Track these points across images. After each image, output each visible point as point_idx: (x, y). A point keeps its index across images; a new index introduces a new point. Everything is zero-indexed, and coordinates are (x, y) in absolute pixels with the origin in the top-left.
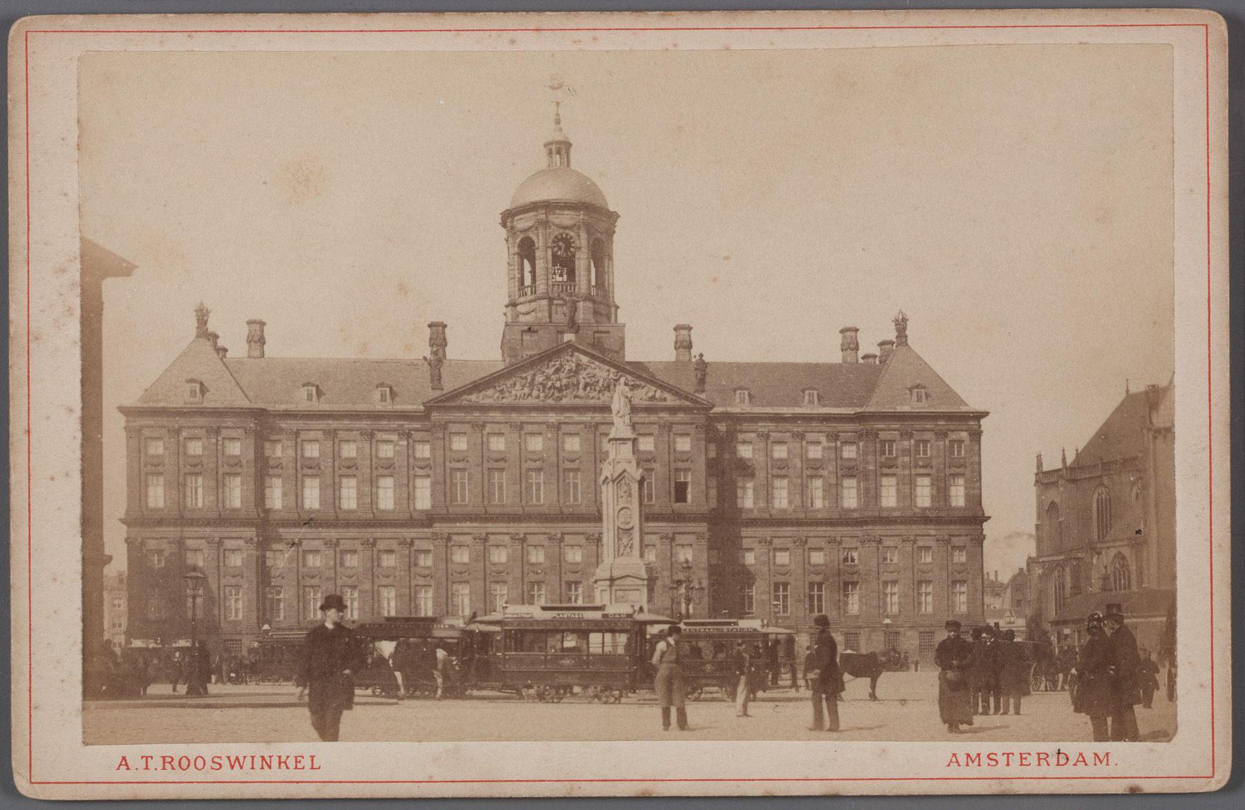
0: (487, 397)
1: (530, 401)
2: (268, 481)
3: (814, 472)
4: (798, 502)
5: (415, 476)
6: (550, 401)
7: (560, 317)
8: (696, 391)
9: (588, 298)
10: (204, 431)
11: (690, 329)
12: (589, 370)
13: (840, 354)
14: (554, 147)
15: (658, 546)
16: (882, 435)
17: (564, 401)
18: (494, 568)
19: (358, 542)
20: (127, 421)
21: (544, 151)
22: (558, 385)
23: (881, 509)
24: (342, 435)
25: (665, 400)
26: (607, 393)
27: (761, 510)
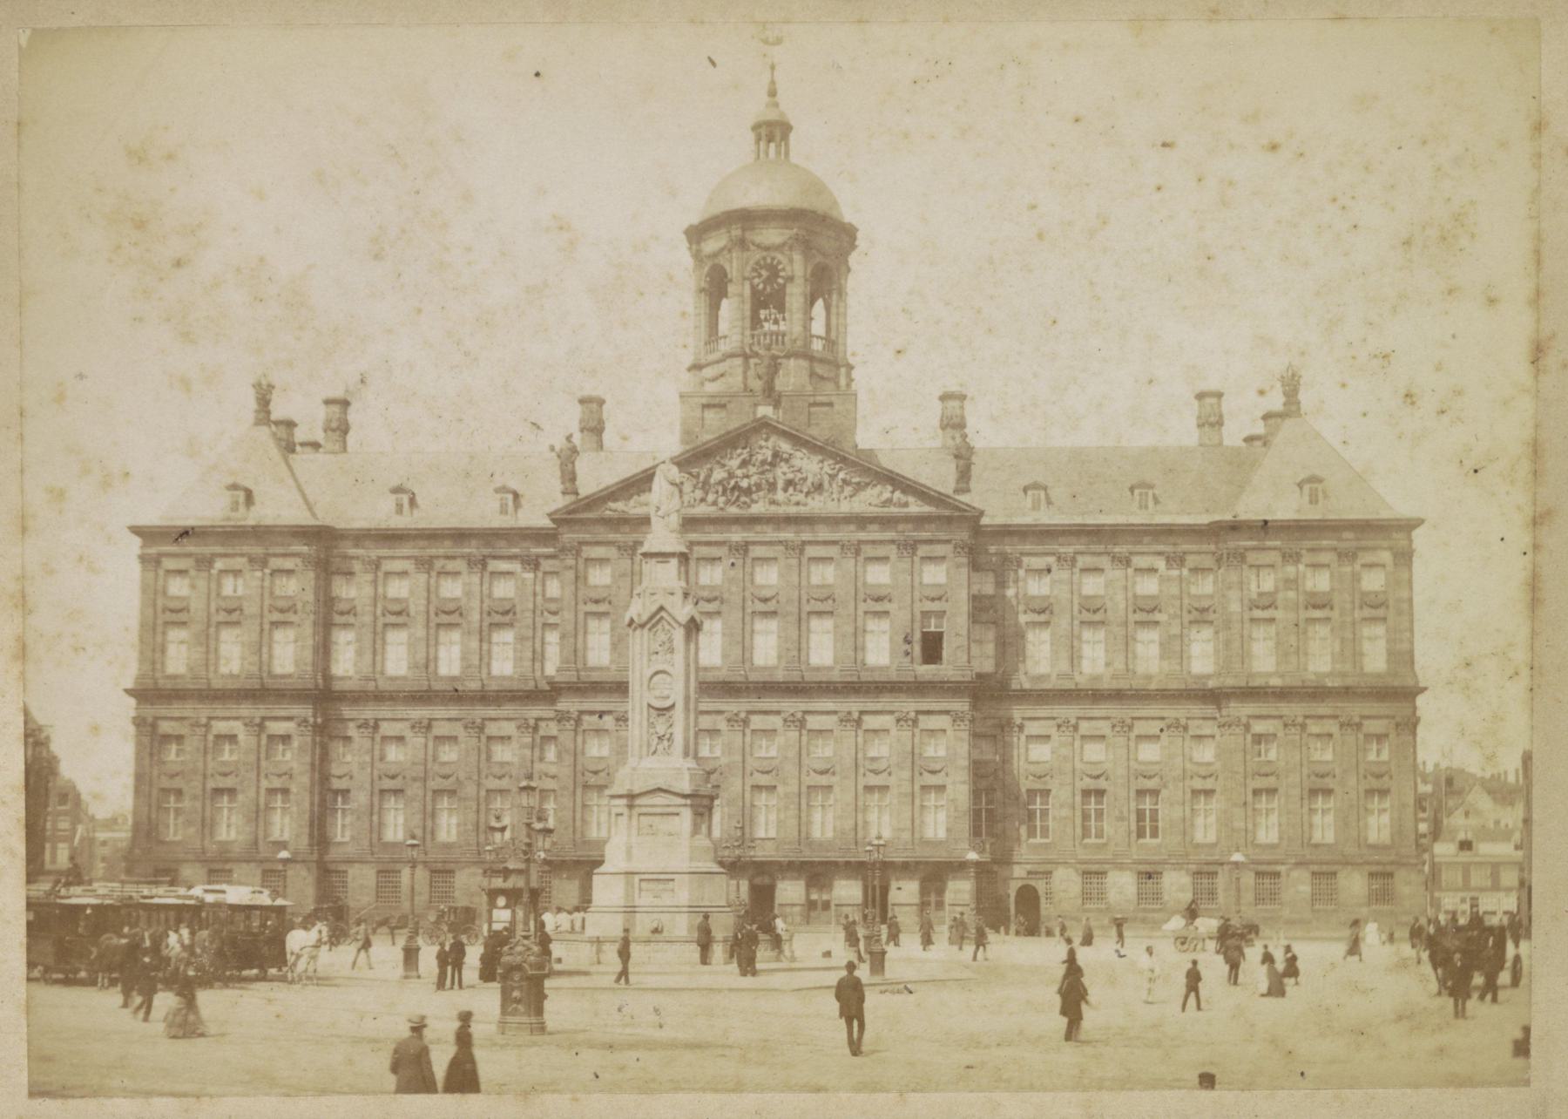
1: (701, 510)
4: (1119, 665)
6: (733, 510)
7: (757, 385)
8: (956, 491)
10: (244, 560)
13: (1196, 433)
14: (763, 131)
16: (1252, 557)
19: (459, 724)
21: (751, 136)
22: (744, 484)
23: (1251, 675)
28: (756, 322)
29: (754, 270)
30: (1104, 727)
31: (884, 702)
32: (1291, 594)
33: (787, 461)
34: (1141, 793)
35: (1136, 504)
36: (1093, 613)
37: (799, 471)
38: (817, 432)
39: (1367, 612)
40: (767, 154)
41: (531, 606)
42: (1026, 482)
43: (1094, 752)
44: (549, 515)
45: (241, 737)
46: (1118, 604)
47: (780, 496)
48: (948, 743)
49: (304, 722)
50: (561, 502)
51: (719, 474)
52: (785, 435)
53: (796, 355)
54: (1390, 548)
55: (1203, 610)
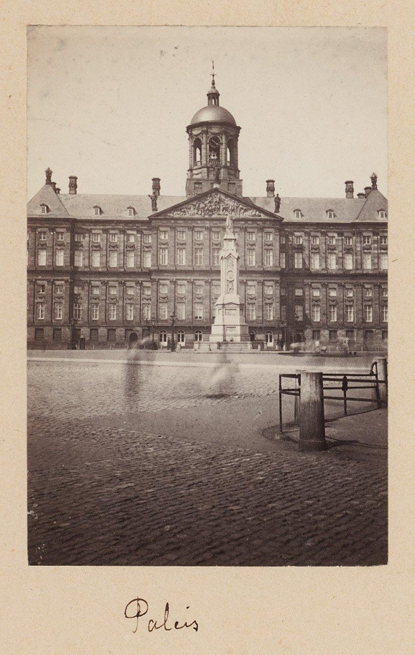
0: (176, 215)
2: (76, 253)
3: (330, 251)
4: (324, 266)
5: (144, 251)
6: (207, 216)
7: (212, 177)
9: (225, 167)
11: (273, 181)
15: (256, 286)
17: (213, 216)
18: (180, 296)
21: (207, 97)
22: (210, 209)
25: (260, 216)
29: (210, 141)
31: (254, 277)
33: (223, 202)
36: (316, 250)
37: (227, 205)
38: (231, 192)
40: (212, 103)
41: (140, 245)
46: (323, 247)
47: (221, 212)
49: (66, 281)
51: (202, 205)
52: (223, 193)
55: (349, 250)
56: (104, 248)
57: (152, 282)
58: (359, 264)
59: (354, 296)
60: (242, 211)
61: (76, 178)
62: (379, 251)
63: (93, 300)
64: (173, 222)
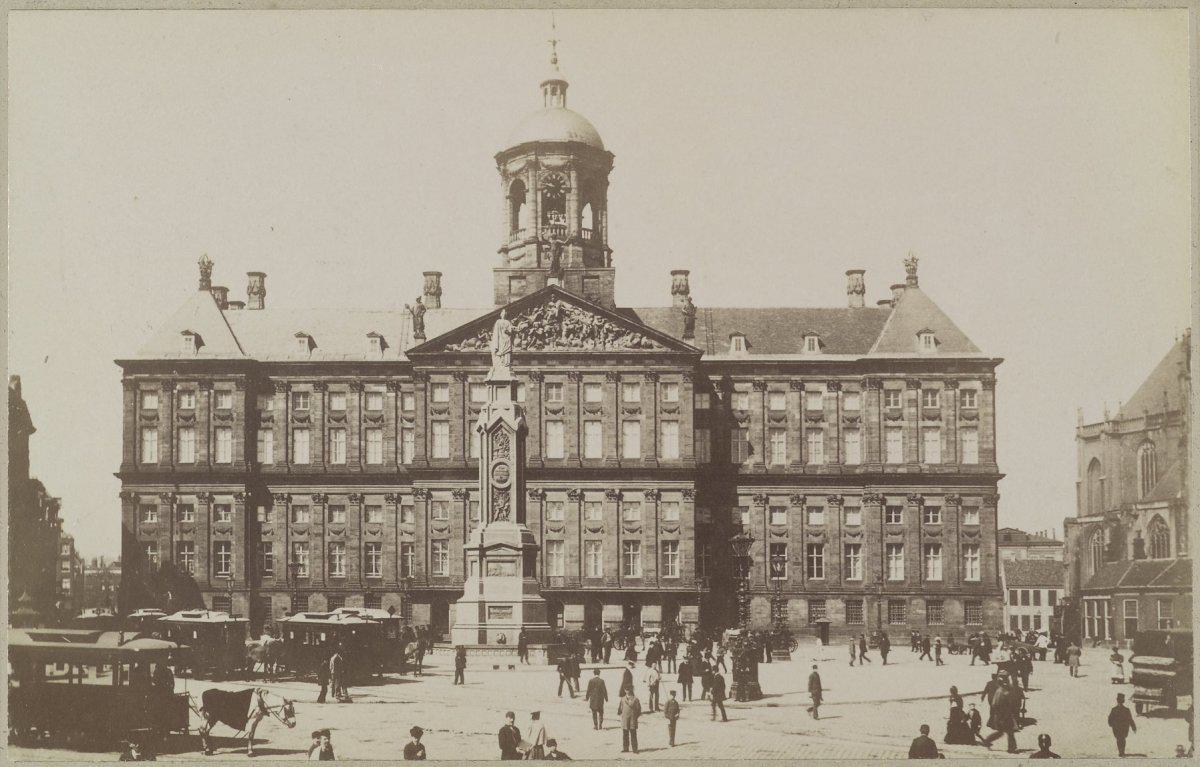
2: (260, 433)
4: (796, 457)
5: (403, 428)
6: (532, 350)
7: (547, 263)
11: (686, 273)
12: (573, 316)
15: (643, 503)
16: (887, 385)
20: (125, 374)
22: (540, 331)
24: (333, 387)
26: (591, 341)
27: (757, 465)
28: (545, 221)
30: (786, 501)
32: (913, 410)
33: (569, 316)
34: (810, 547)
35: (806, 346)
36: (777, 422)
37: (577, 323)
39: (964, 423)
42: (733, 330)
43: (779, 518)
44: (406, 353)
45: (196, 506)
47: (564, 340)
48: (678, 510)
49: (238, 496)
50: (413, 344)
51: (523, 325)
53: (573, 241)
54: (980, 379)
55: (853, 420)
56: (318, 424)
57: (415, 495)
58: (878, 449)
59: (863, 521)
60: (611, 336)
61: (262, 276)
62: (921, 424)
63: (296, 535)
64: (458, 362)
